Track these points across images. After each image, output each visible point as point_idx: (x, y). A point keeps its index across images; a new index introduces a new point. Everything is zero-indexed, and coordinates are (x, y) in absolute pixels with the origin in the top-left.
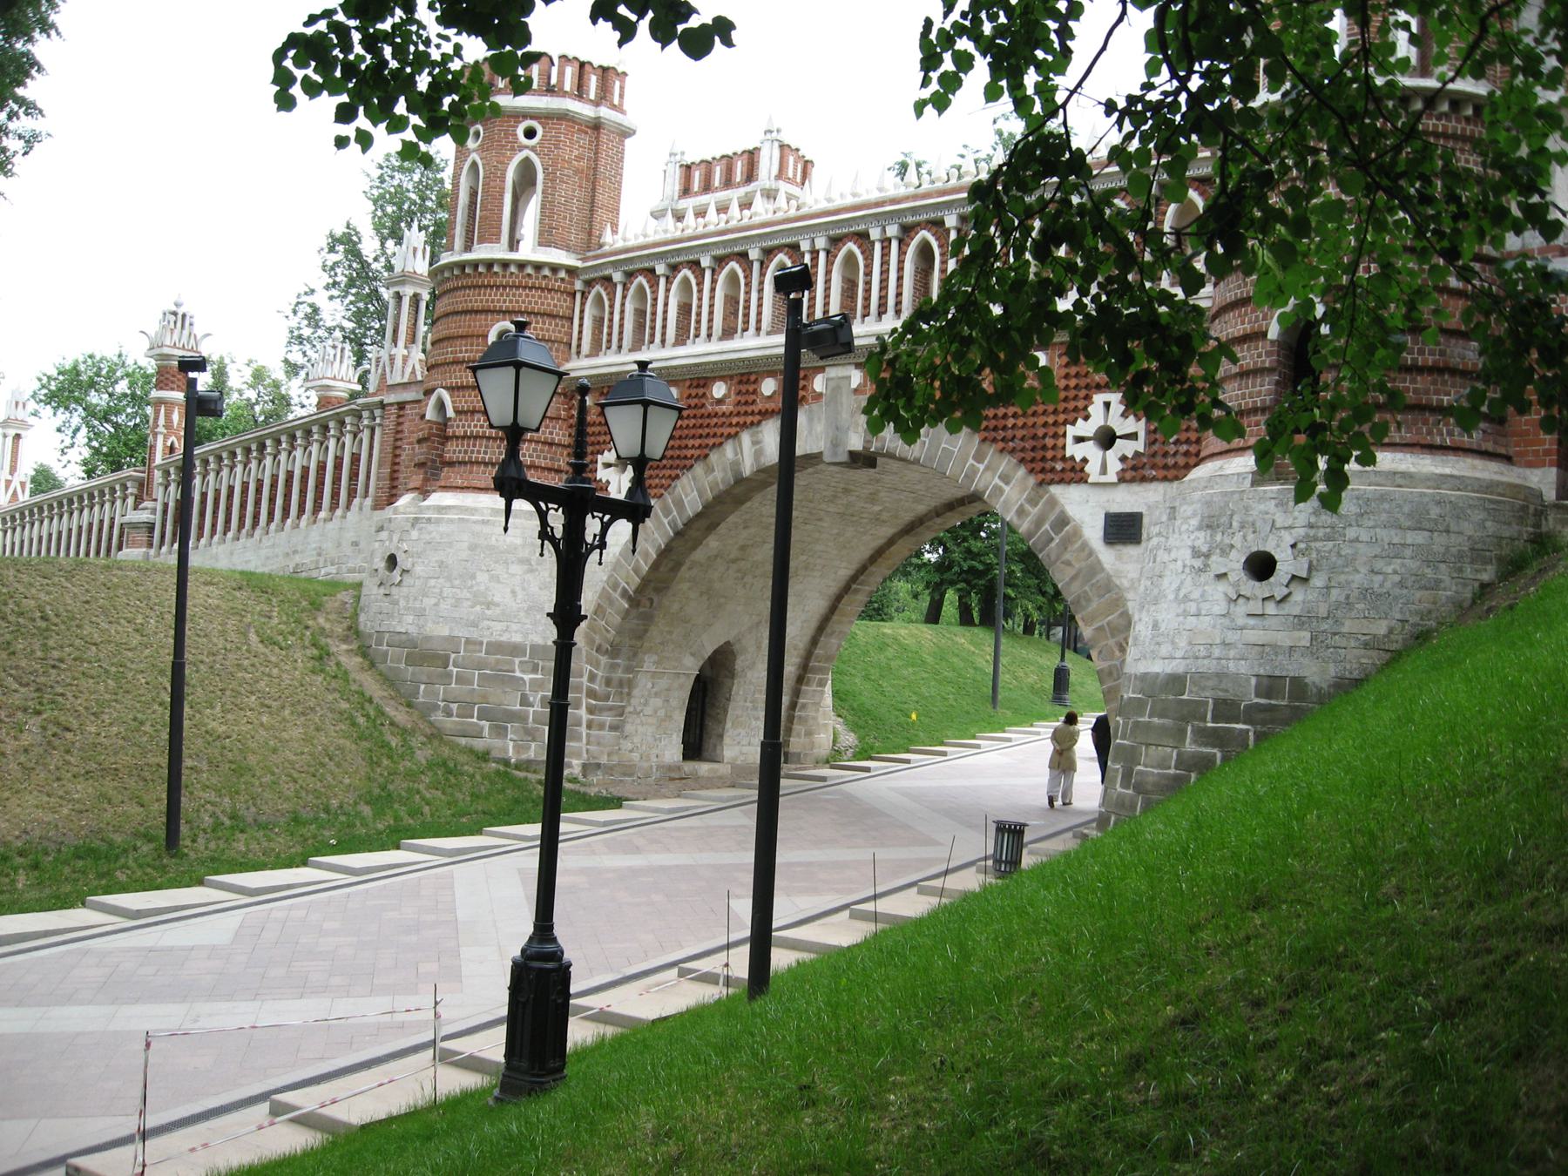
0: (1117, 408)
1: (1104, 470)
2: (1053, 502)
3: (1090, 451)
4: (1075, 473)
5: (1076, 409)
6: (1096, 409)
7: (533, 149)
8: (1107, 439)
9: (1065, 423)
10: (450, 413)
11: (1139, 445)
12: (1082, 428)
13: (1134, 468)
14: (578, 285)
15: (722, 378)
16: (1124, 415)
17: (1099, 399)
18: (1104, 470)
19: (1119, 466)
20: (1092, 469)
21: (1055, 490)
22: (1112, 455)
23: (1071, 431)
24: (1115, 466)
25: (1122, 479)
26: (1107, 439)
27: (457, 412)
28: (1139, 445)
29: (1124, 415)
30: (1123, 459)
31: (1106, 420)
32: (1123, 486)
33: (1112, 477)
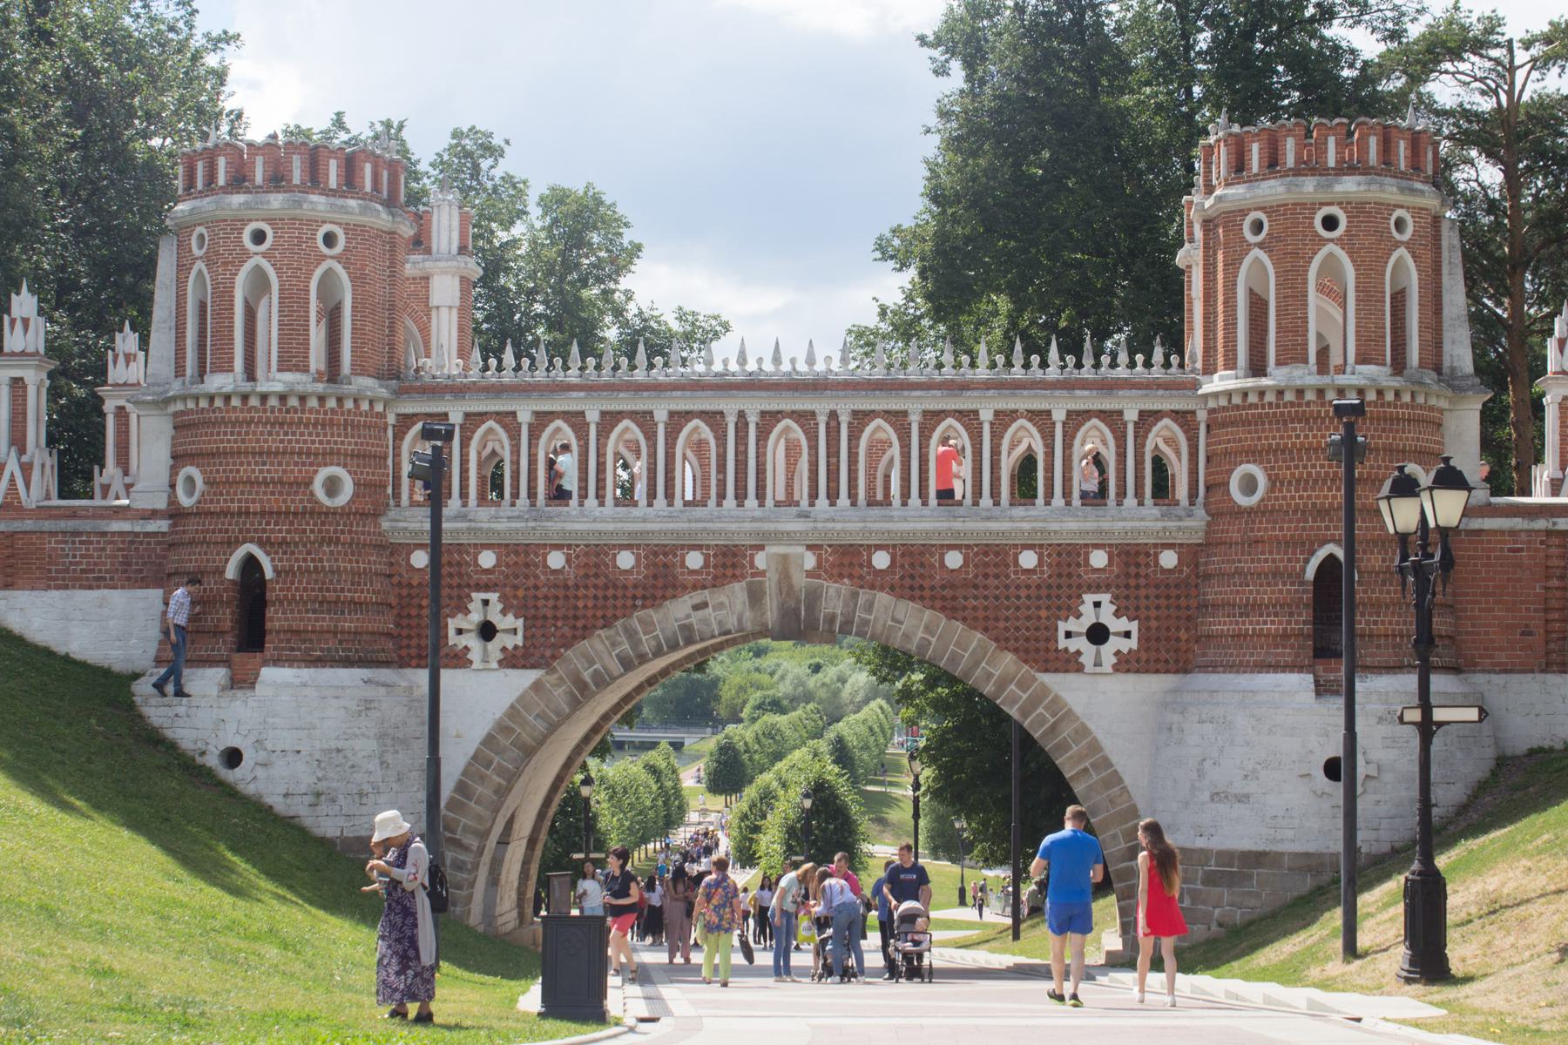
0: (1108, 609)
1: (1098, 664)
2: (1045, 690)
3: (1081, 644)
4: (1070, 664)
5: (1069, 608)
6: (1087, 608)
7: (337, 258)
8: (1098, 634)
9: (1058, 618)
10: (269, 573)
11: (1133, 643)
12: (1072, 625)
13: (1127, 661)
14: (391, 419)
15: (628, 547)
16: (1117, 614)
17: (1089, 598)
18: (1098, 664)
19: (1114, 660)
20: (1087, 659)
21: (1046, 678)
22: (1109, 649)
23: (1063, 627)
24: (1109, 660)
25: (1116, 668)
26: (1098, 634)
27: (275, 569)
28: (1133, 643)
29: (1117, 614)
30: (1118, 653)
31: (1097, 616)
32: (1121, 677)
33: (1107, 667)
